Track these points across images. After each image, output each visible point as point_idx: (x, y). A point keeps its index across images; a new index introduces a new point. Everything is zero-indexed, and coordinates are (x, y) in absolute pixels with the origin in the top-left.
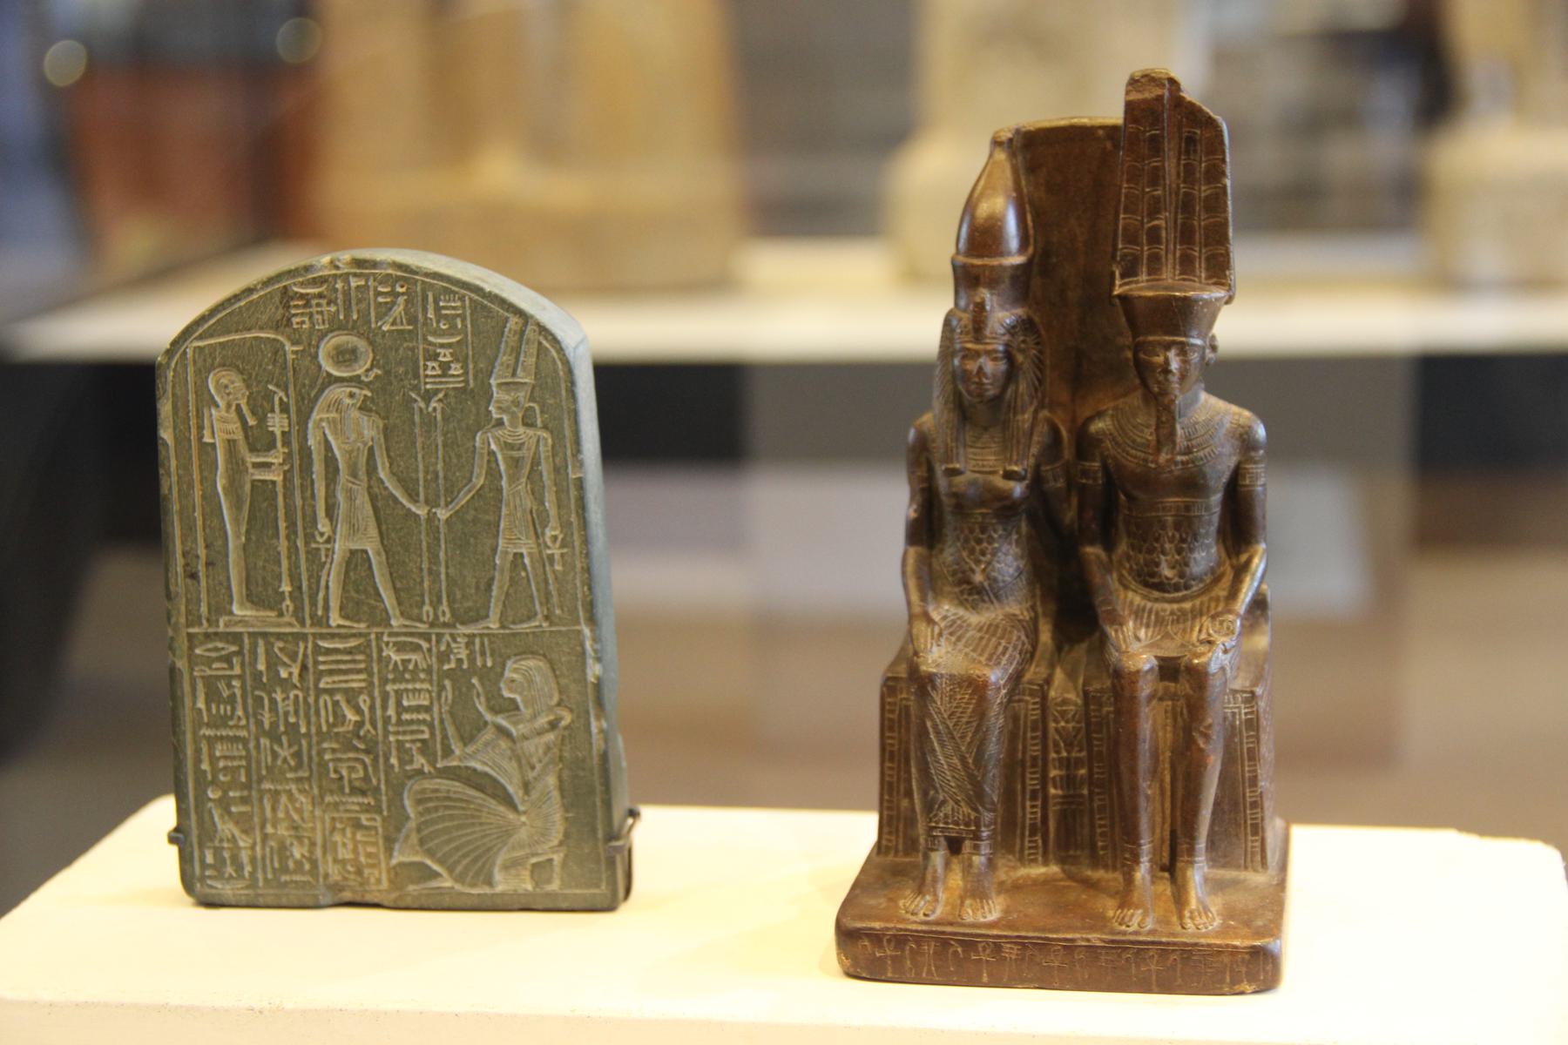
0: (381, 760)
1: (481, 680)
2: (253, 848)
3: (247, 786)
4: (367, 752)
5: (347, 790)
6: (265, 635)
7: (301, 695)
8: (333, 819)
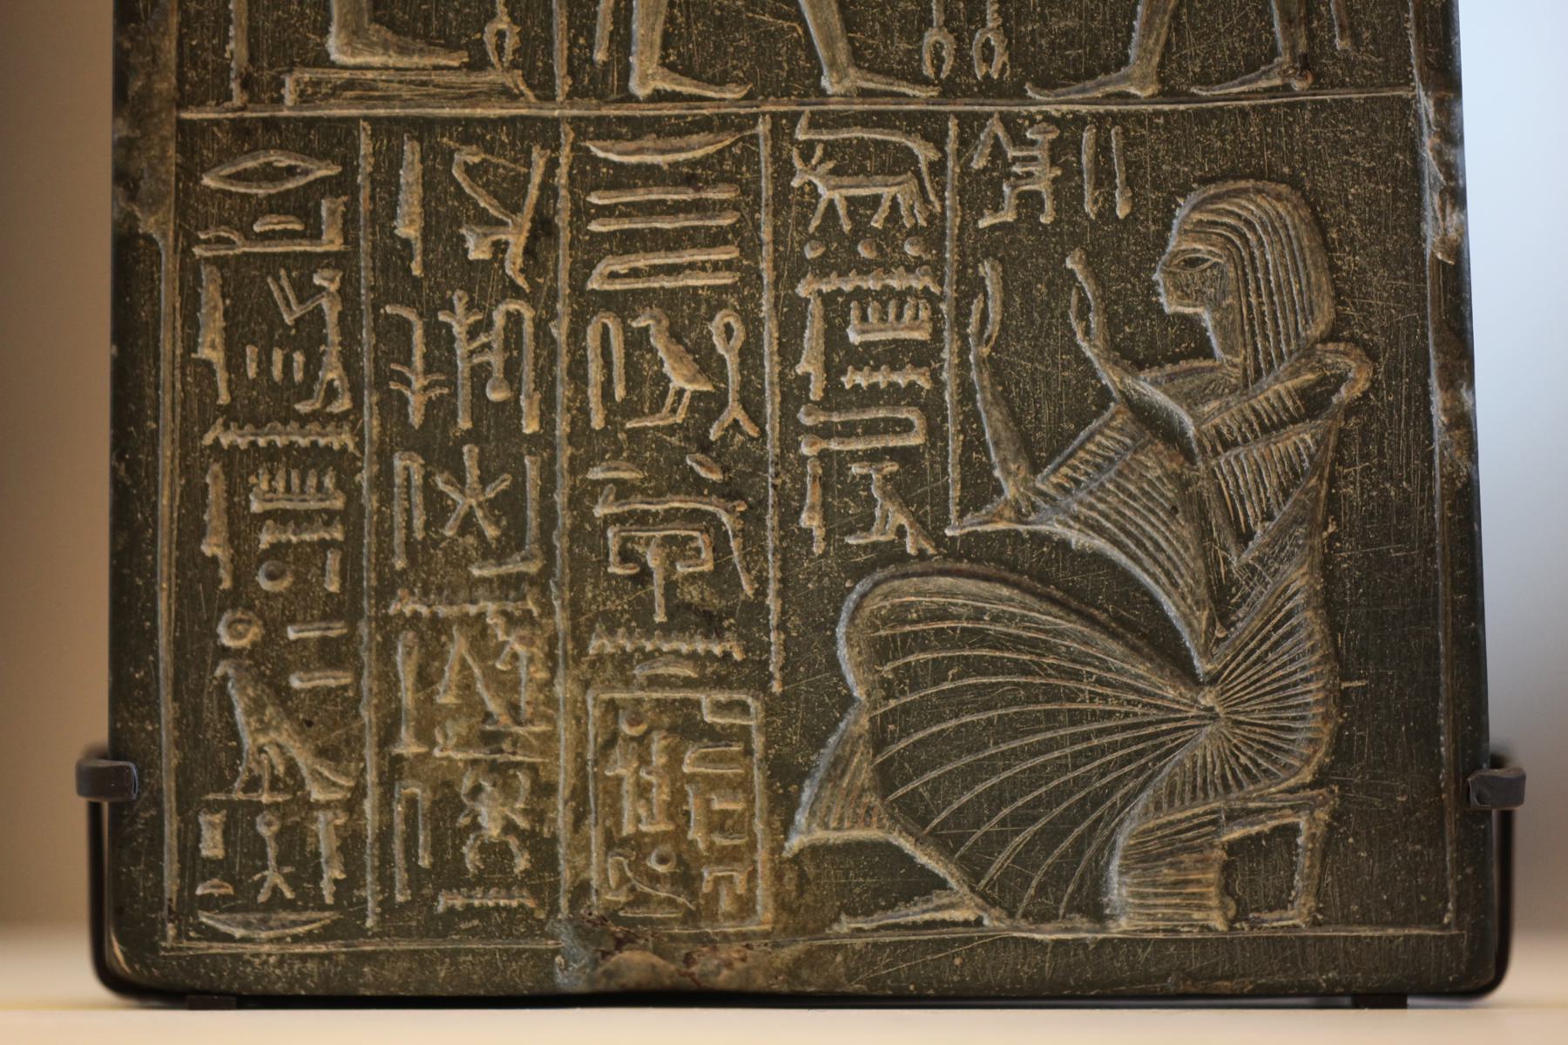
0: (771, 519)
1: (1091, 262)
2: (352, 805)
3: (344, 608)
4: (728, 492)
5: (660, 617)
6: (423, 128)
7: (528, 314)
8: (612, 707)
